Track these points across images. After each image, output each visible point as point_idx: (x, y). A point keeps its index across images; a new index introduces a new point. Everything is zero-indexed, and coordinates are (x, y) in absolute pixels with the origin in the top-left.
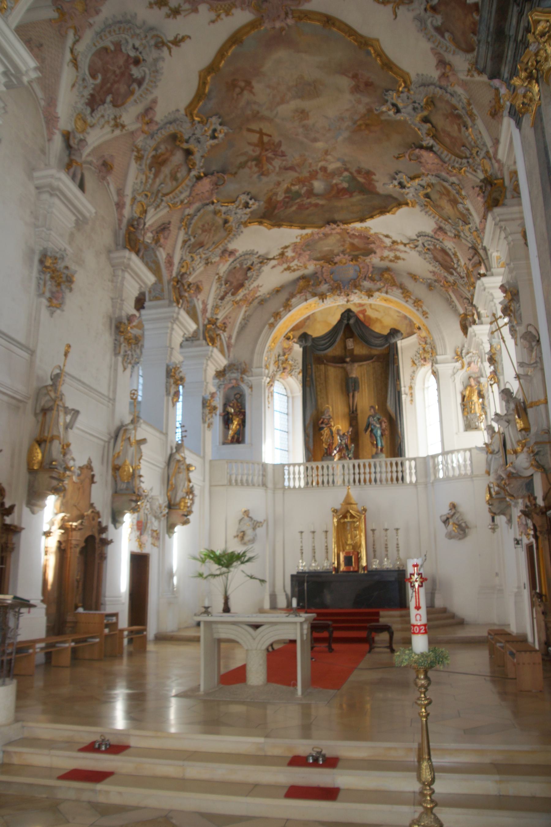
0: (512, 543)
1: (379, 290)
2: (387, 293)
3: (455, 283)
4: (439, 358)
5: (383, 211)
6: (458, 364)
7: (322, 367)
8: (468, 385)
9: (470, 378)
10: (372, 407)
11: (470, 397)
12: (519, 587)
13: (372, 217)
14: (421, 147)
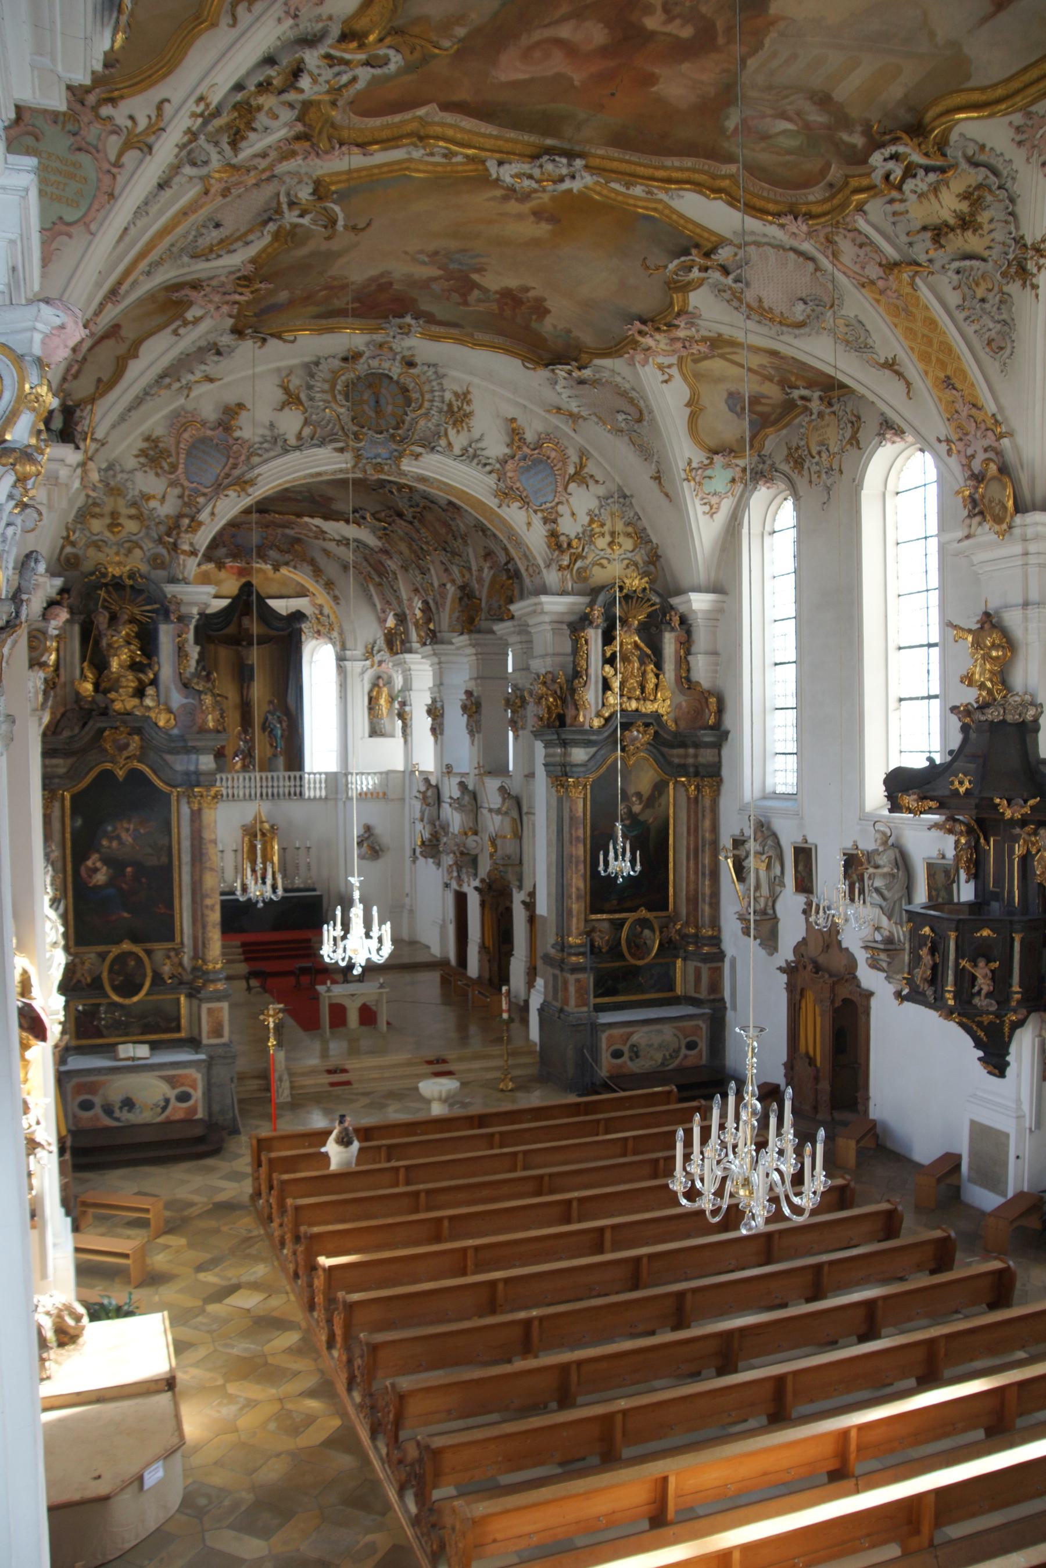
0: (441, 886)
1: (287, 564)
2: (295, 567)
3: (380, 584)
4: (348, 653)
5: (326, 518)
6: (368, 663)
7: (212, 646)
8: (375, 685)
9: (379, 677)
10: (271, 702)
11: (377, 699)
12: (444, 920)
13: (312, 517)
14: (400, 515)
